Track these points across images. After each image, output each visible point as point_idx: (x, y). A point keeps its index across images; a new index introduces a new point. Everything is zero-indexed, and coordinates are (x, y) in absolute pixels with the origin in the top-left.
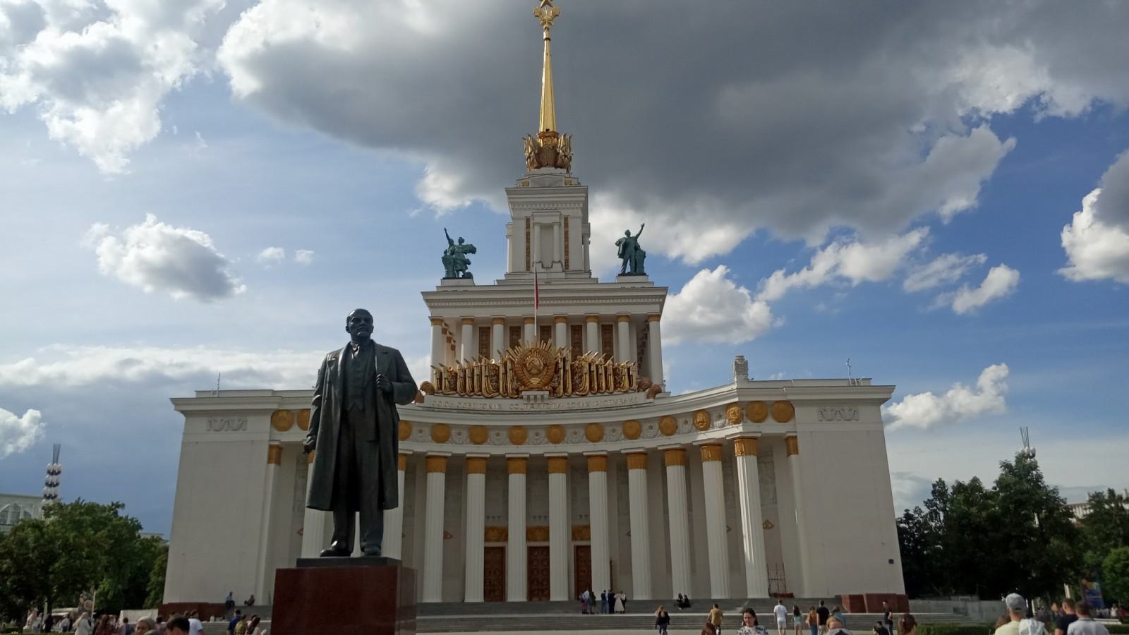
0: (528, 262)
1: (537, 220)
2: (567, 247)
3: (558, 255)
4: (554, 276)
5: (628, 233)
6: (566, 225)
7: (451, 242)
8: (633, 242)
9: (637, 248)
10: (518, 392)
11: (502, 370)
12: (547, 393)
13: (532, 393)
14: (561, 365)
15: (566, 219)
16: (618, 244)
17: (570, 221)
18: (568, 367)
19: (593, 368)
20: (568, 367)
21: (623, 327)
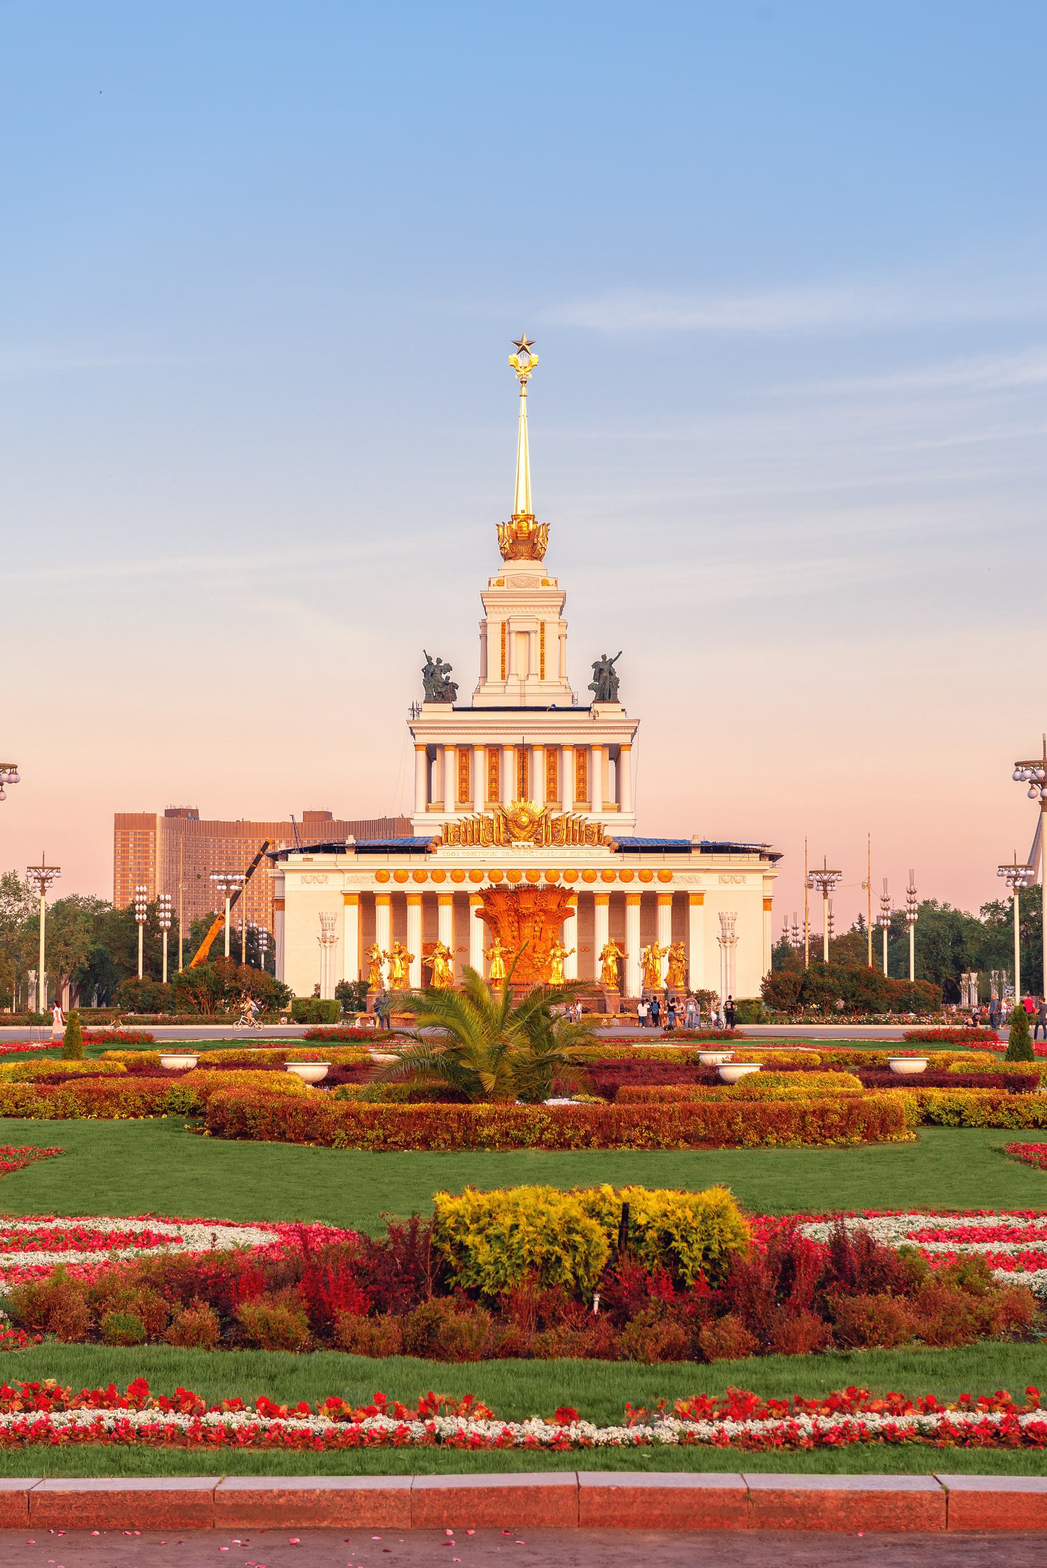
0: (503, 671)
1: (514, 627)
2: (542, 655)
3: (536, 668)
4: (528, 690)
5: (604, 657)
6: (542, 630)
7: (429, 659)
8: (606, 667)
9: (611, 673)
10: (509, 841)
11: (495, 825)
12: (532, 844)
13: (520, 844)
14: (543, 822)
15: (542, 624)
16: (595, 666)
17: (546, 626)
18: (549, 824)
19: (570, 825)
20: (549, 824)
21: (597, 755)
